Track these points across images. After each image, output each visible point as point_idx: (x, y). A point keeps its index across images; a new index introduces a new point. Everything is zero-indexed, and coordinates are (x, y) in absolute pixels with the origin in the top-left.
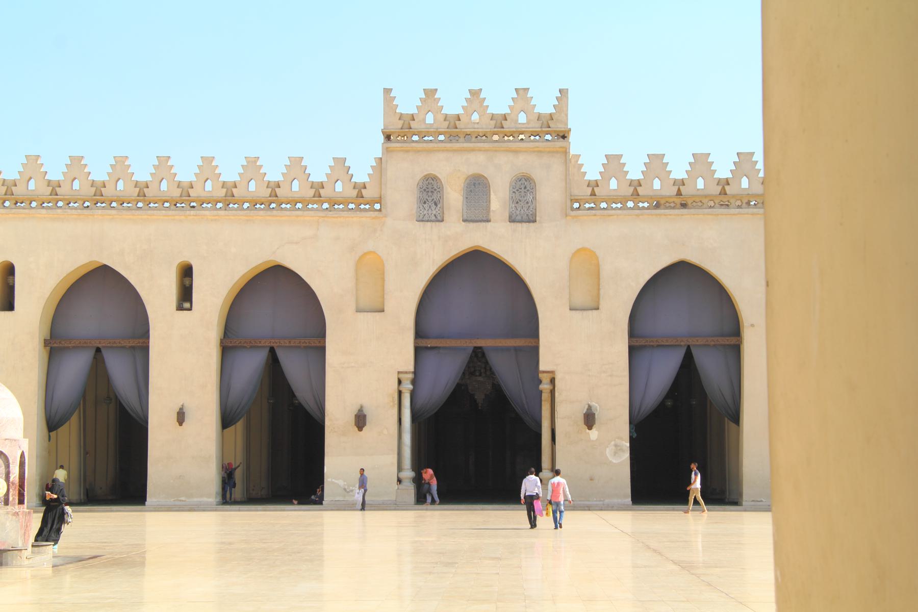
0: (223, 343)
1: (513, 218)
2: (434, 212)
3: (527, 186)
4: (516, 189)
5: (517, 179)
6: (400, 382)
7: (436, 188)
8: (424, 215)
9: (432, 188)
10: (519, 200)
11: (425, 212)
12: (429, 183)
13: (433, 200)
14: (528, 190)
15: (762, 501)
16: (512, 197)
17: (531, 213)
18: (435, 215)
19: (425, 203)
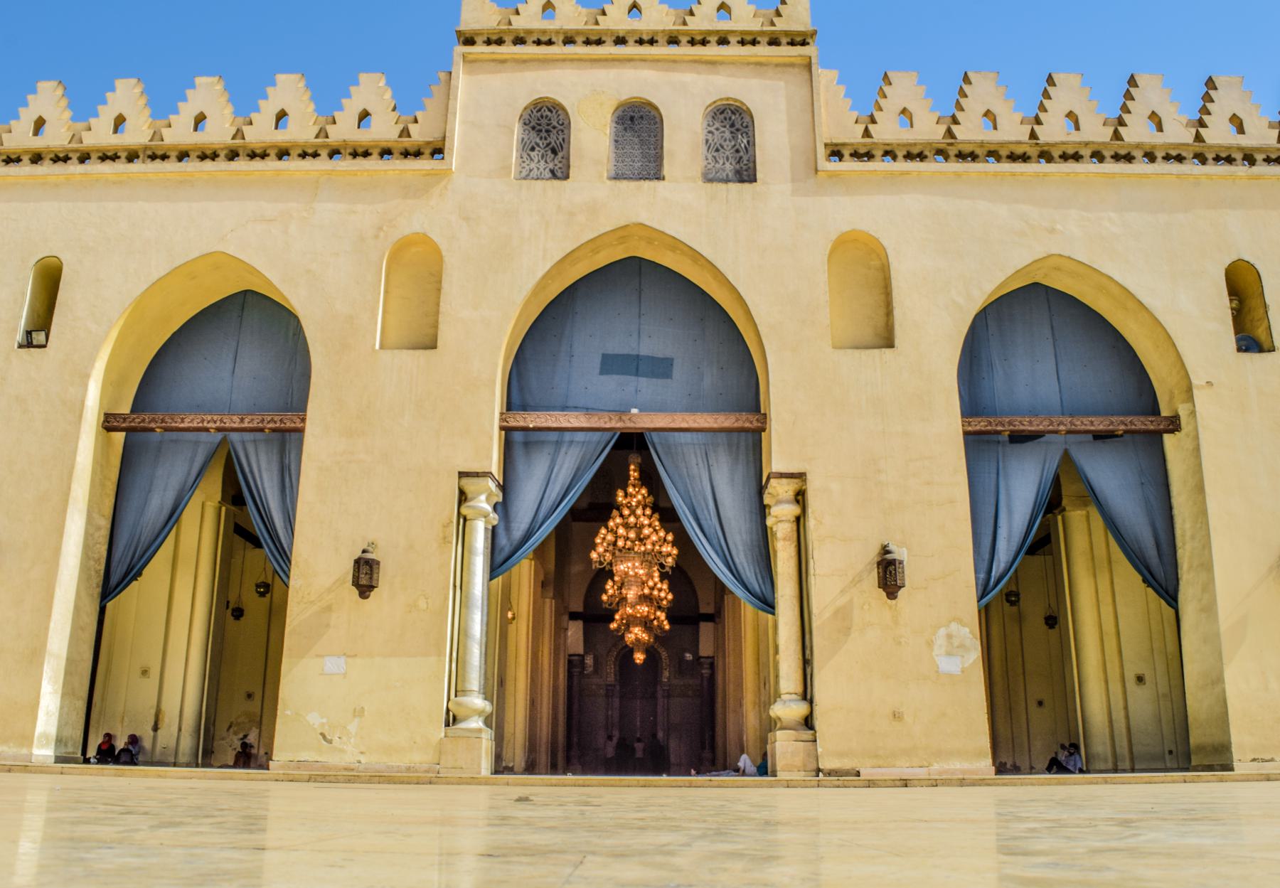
0: (108, 422)
1: (710, 176)
2: (551, 166)
3: (736, 124)
4: (715, 127)
5: (715, 110)
6: (463, 497)
7: (555, 123)
8: (531, 170)
9: (548, 125)
10: (720, 145)
11: (533, 165)
12: (542, 117)
13: (548, 145)
14: (738, 130)
15: (1272, 760)
16: (707, 141)
17: (745, 167)
18: (552, 171)
19: (533, 149)
